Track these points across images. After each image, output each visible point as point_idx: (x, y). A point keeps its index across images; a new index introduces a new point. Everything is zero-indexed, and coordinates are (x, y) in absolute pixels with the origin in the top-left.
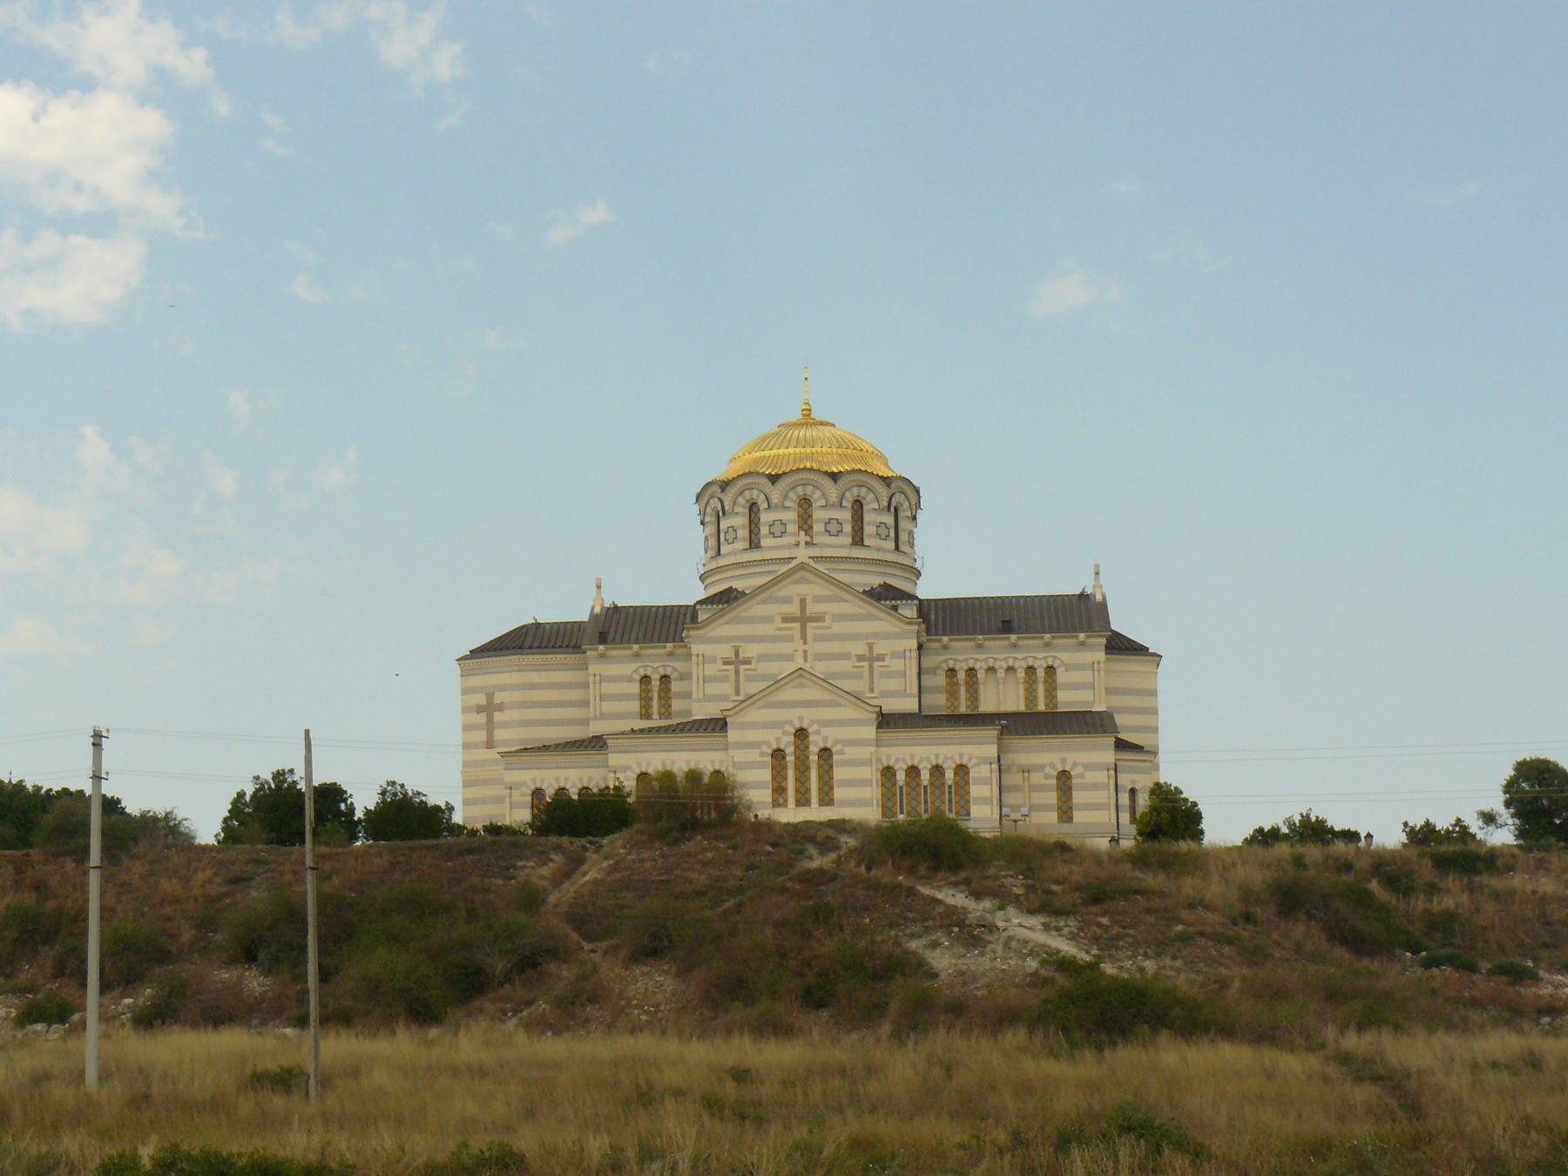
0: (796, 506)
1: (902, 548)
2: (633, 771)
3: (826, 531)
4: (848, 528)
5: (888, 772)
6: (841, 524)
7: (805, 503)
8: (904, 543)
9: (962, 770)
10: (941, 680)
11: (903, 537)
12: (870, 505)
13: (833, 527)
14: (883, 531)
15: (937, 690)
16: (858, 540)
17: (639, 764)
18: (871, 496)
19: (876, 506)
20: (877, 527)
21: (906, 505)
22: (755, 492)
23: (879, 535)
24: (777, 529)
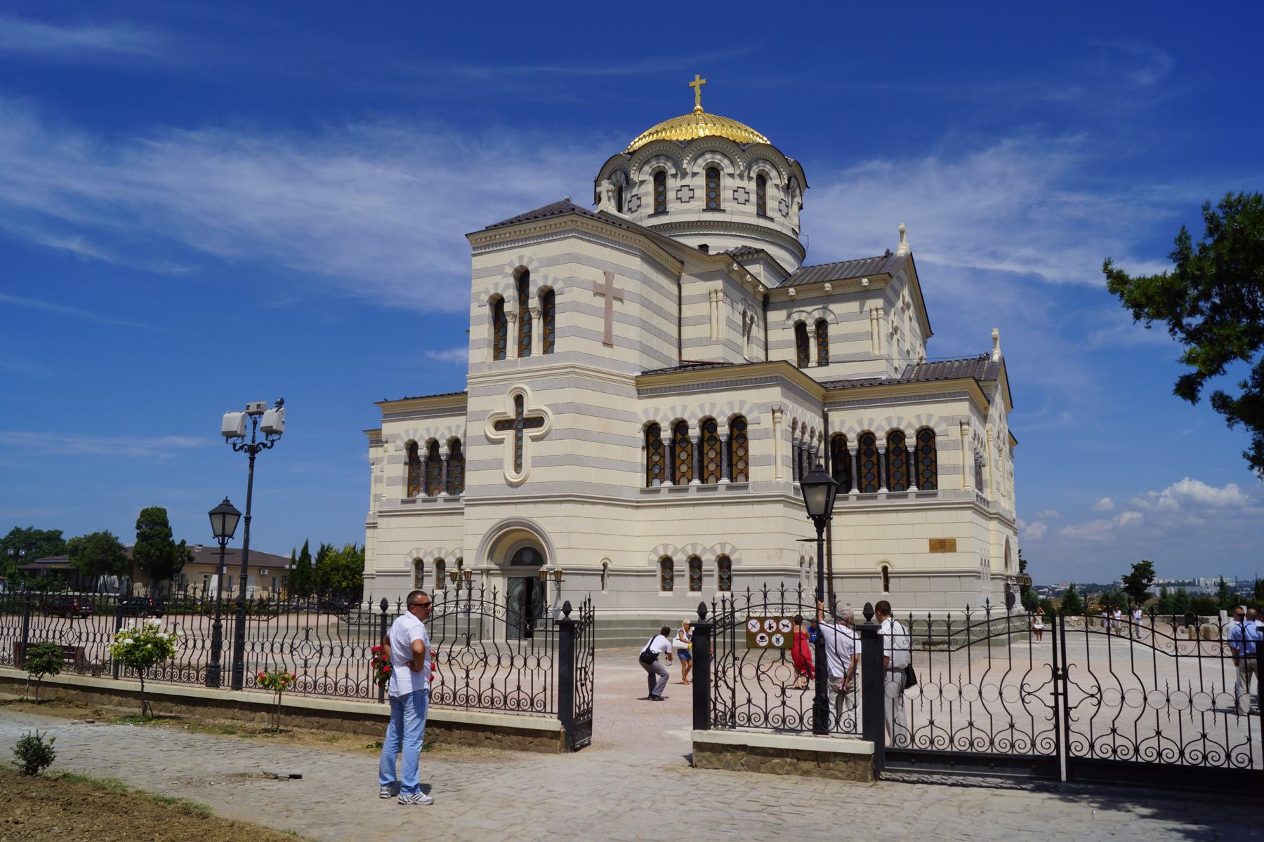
0: (651, 179)
1: (769, 214)
2: (402, 440)
3: (678, 199)
4: (701, 193)
5: (652, 430)
6: (693, 190)
7: (660, 177)
8: (773, 209)
9: (738, 423)
10: (791, 334)
11: (771, 204)
12: (727, 167)
13: (685, 194)
14: (741, 196)
15: (783, 345)
16: (713, 203)
17: (407, 432)
18: (725, 163)
19: (731, 170)
20: (734, 191)
21: (774, 173)
22: (619, 173)
23: (737, 199)
24: (635, 202)
